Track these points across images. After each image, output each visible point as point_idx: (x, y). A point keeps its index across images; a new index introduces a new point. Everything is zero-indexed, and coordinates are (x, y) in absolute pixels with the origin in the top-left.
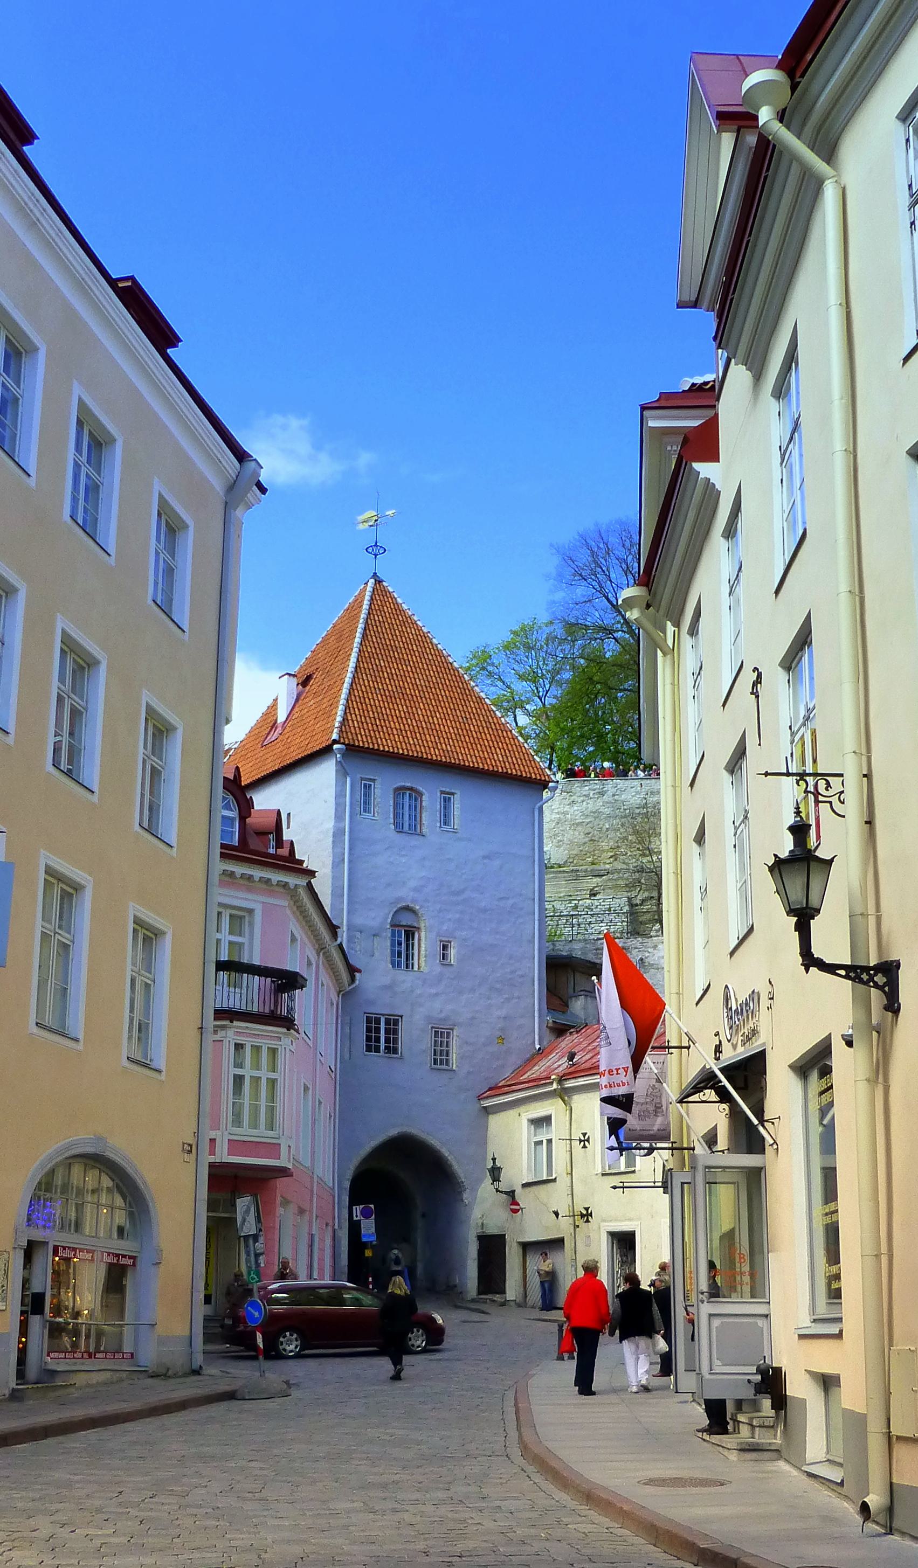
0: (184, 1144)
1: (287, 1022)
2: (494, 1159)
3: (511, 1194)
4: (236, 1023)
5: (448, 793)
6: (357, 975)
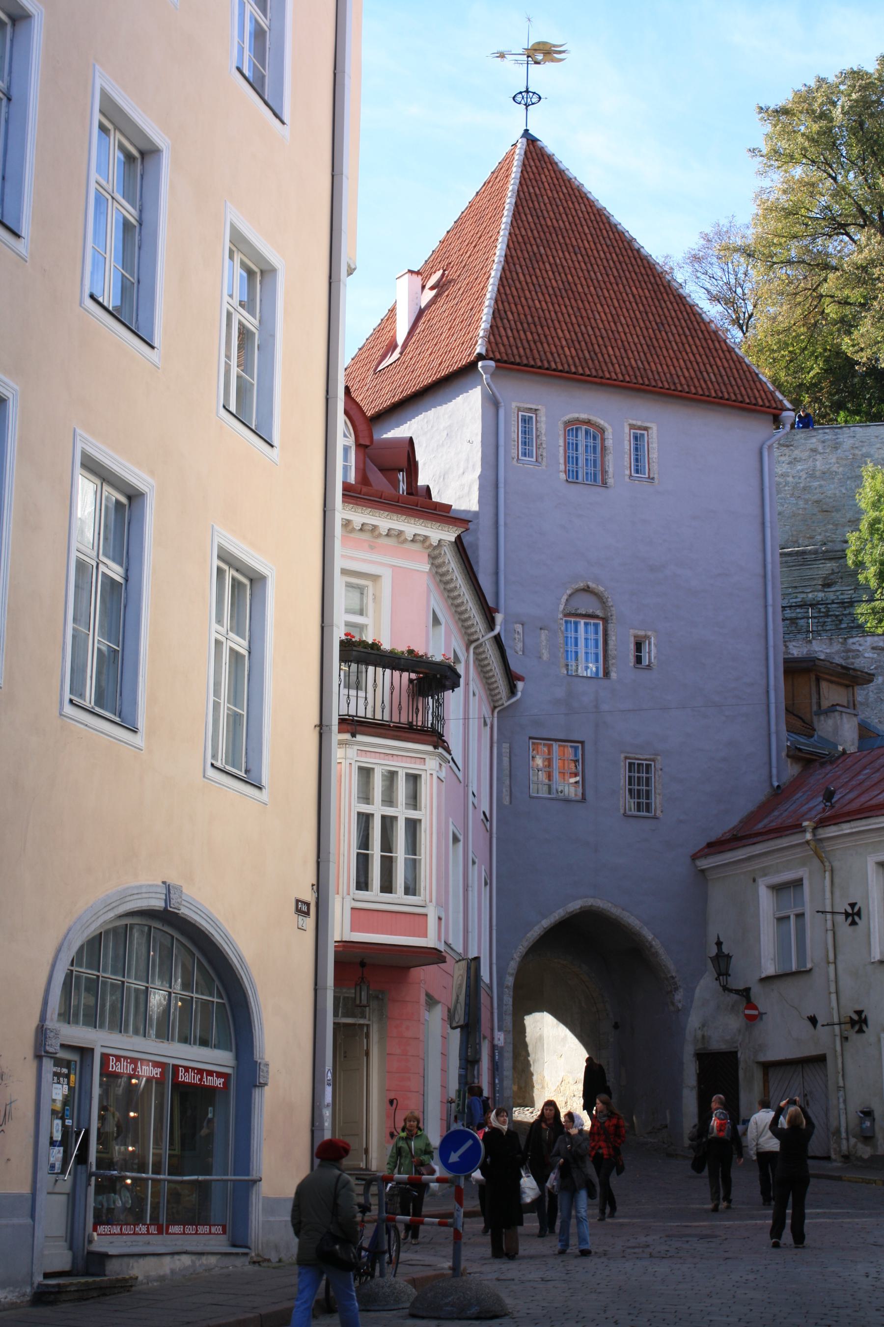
0: (297, 901)
1: (435, 737)
2: (719, 944)
3: (746, 993)
4: (359, 738)
5: (640, 428)
6: (520, 685)
